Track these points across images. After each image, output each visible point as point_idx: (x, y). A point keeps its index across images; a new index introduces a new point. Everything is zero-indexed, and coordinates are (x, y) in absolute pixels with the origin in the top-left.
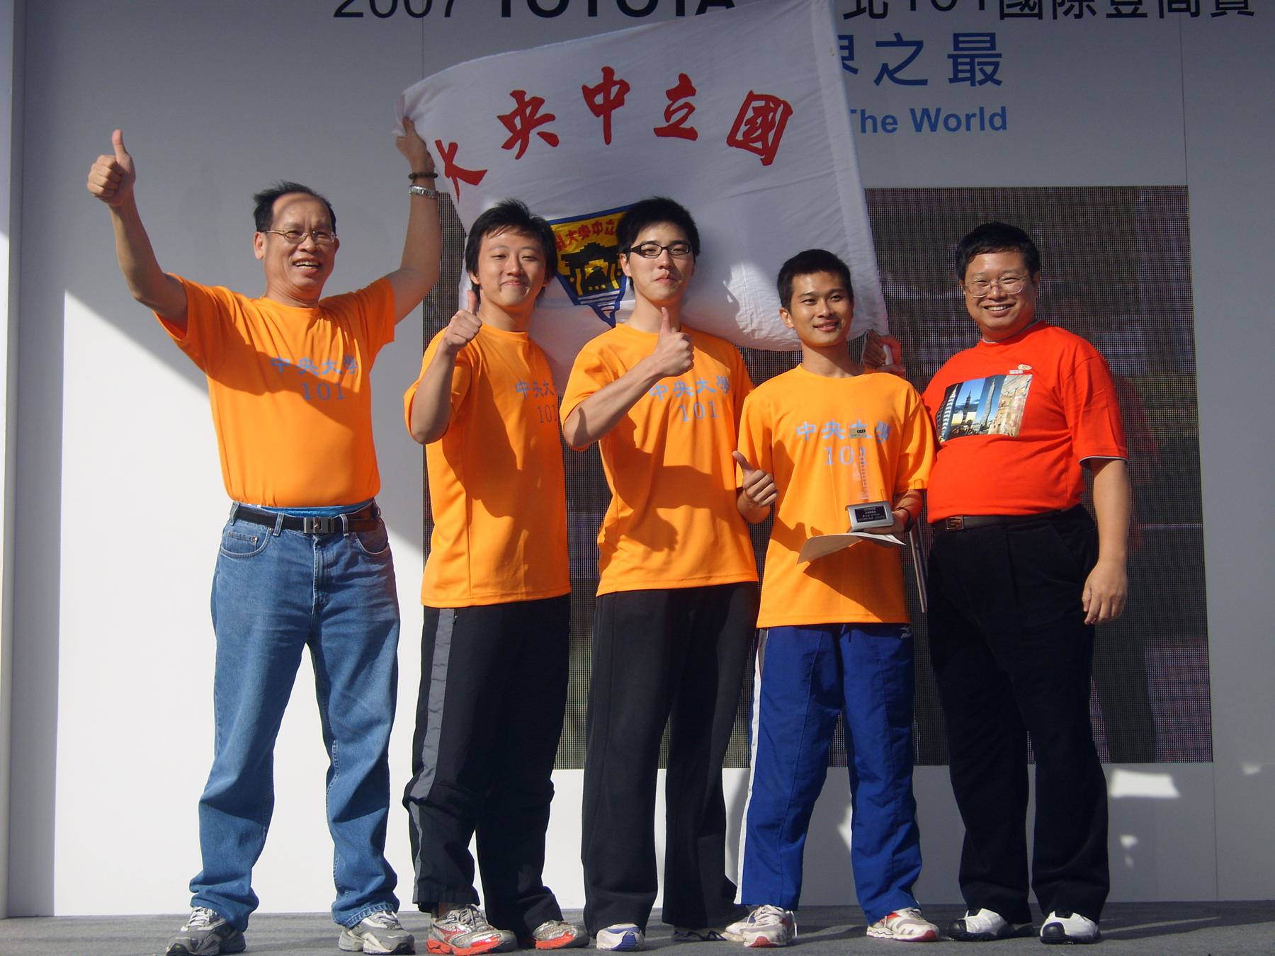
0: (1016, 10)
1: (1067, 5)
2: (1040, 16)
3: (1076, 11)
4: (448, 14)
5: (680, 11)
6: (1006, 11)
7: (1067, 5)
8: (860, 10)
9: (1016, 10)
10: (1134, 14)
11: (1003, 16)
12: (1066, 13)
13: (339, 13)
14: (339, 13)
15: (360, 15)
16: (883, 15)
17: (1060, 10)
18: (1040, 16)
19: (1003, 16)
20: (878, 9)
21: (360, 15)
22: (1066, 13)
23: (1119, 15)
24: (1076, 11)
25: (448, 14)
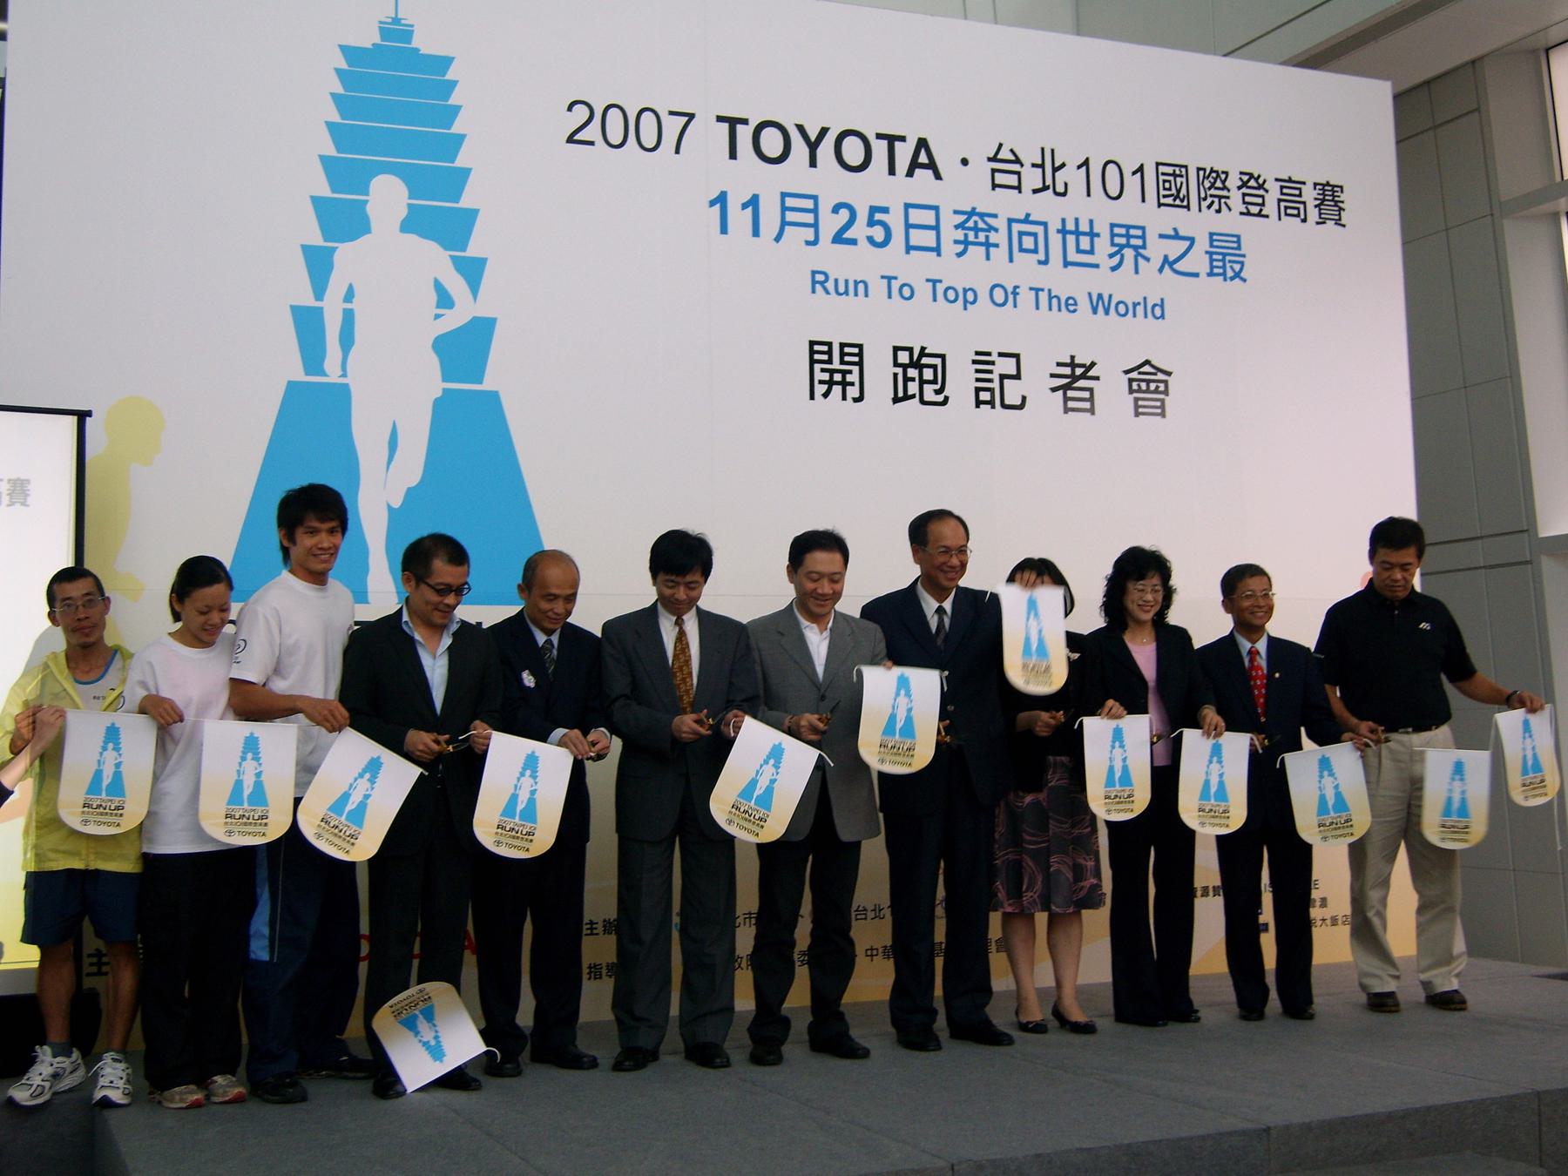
0: (1169, 201)
1: (1209, 200)
2: (1188, 207)
3: (1216, 206)
4: (677, 152)
5: (892, 171)
6: (1163, 201)
7: (1209, 200)
8: (1045, 188)
9: (1169, 201)
10: (1259, 215)
11: (1160, 205)
12: (1209, 207)
13: (570, 140)
14: (570, 140)
15: (592, 143)
16: (1064, 194)
17: (1205, 204)
18: (1188, 207)
19: (1160, 205)
20: (1060, 189)
21: (592, 143)
22: (1209, 207)
23: (1248, 213)
24: (1216, 206)
25: (677, 152)
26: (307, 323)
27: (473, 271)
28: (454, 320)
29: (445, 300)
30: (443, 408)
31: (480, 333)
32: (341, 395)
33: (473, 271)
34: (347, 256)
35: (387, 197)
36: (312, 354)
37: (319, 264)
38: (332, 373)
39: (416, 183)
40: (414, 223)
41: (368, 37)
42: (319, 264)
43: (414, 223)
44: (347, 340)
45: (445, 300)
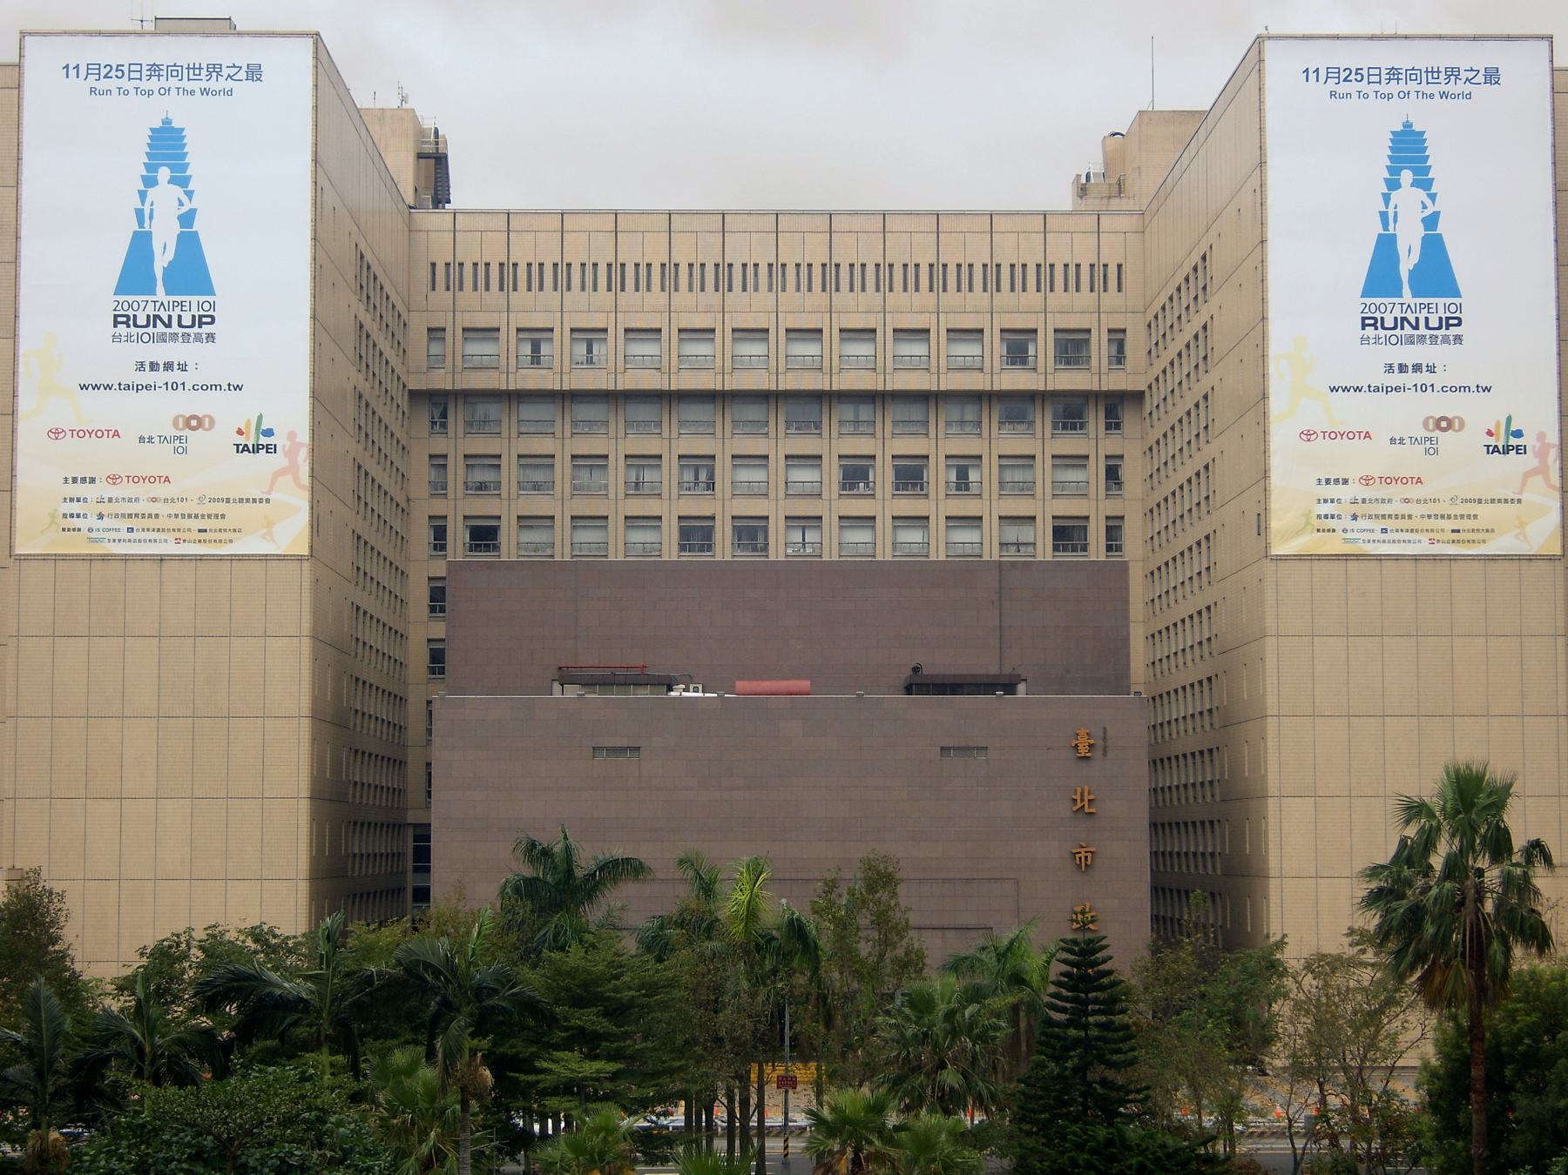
26: (139, 214)
27: (190, 194)
28: (184, 210)
29: (181, 204)
30: (181, 237)
31: (192, 212)
32: (149, 234)
33: (190, 194)
34: (151, 192)
35: (164, 173)
36: (141, 222)
37: (143, 195)
38: (147, 228)
39: (173, 168)
40: (172, 181)
41: (158, 125)
42: (143, 195)
43: (172, 181)
44: (151, 218)
45: (181, 204)
